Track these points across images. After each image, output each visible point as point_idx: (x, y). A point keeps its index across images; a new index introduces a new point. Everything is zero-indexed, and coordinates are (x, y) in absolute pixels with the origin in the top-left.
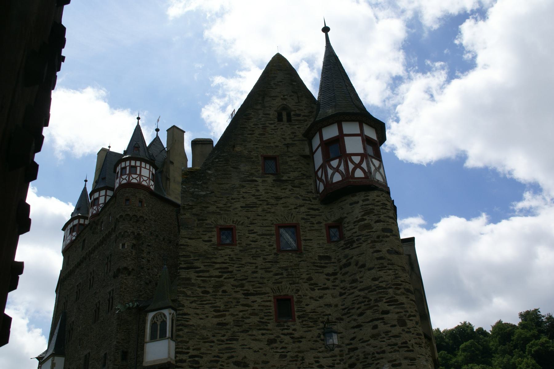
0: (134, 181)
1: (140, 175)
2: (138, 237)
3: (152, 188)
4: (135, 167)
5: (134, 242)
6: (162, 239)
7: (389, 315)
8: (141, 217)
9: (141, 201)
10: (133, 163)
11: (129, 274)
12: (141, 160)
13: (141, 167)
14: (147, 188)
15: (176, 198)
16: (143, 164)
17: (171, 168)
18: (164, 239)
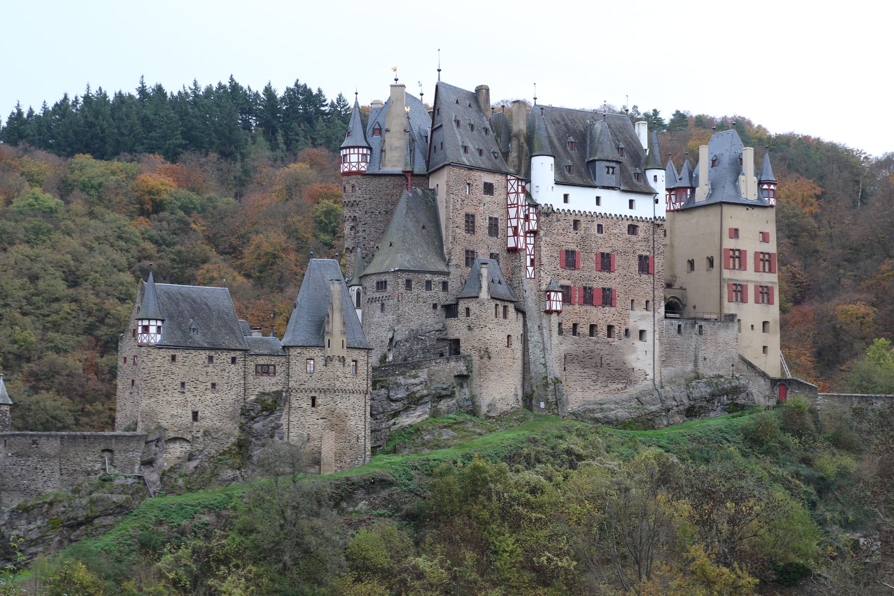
0: (346, 170)
1: (350, 163)
2: (354, 219)
3: (363, 169)
4: (346, 155)
5: (352, 224)
6: (377, 213)
7: (378, 312)
8: (355, 201)
9: (353, 187)
10: (345, 153)
11: (351, 252)
12: (349, 147)
13: (350, 154)
14: (359, 173)
15: (393, 166)
16: (352, 150)
17: (387, 136)
18: (380, 213)
